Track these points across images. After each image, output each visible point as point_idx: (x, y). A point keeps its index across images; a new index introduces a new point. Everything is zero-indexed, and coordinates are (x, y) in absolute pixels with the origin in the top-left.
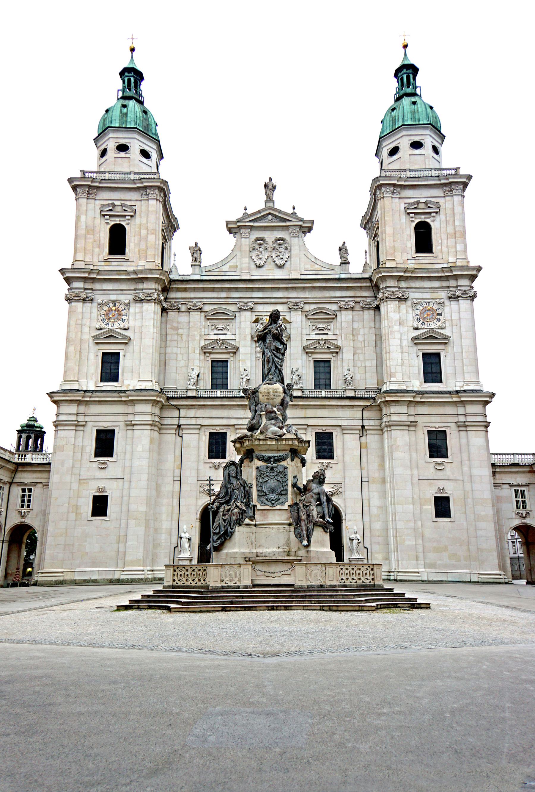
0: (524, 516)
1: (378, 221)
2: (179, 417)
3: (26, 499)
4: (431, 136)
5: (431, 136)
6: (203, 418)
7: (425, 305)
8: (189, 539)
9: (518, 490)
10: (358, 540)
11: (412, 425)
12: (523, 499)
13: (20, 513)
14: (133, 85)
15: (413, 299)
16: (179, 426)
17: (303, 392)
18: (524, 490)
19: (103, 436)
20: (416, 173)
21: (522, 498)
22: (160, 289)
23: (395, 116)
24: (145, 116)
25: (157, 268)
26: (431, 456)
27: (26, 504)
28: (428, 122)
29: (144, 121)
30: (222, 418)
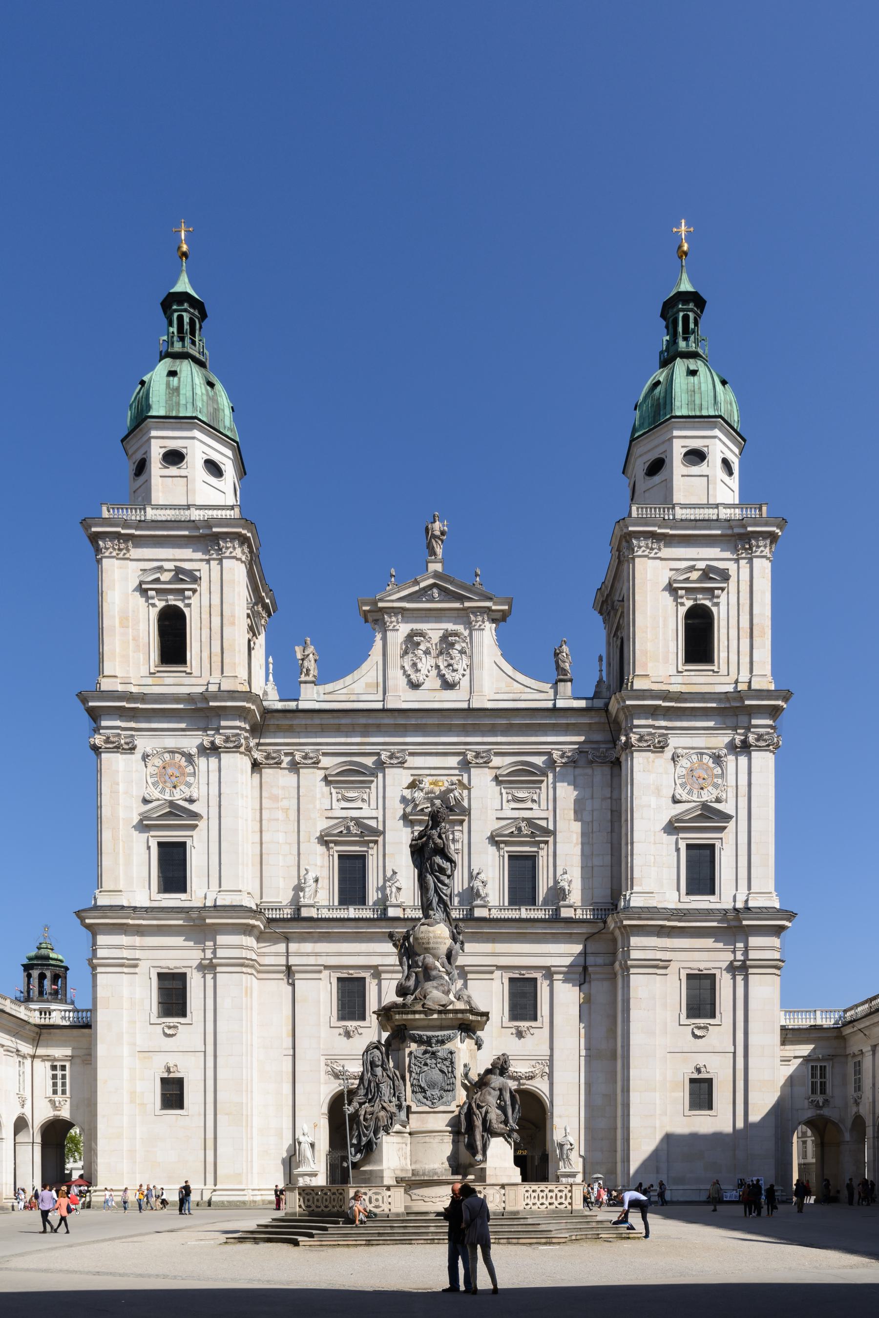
0: (821, 1104)
1: (623, 601)
2: (287, 952)
3: (59, 1082)
4: (720, 440)
5: (720, 440)
6: (328, 954)
7: (694, 757)
8: (312, 1145)
9: (816, 1066)
10: (571, 1145)
11: (661, 965)
12: (823, 1080)
13: (52, 1102)
14: (186, 327)
15: (675, 748)
16: (289, 968)
17: (490, 910)
18: (825, 1067)
19: (168, 984)
20: (692, 511)
21: (821, 1078)
22: (248, 728)
23: (659, 399)
24: (211, 393)
25: (241, 688)
26: (689, 1016)
27: (59, 1089)
28: (717, 414)
29: (210, 402)
30: (358, 954)
